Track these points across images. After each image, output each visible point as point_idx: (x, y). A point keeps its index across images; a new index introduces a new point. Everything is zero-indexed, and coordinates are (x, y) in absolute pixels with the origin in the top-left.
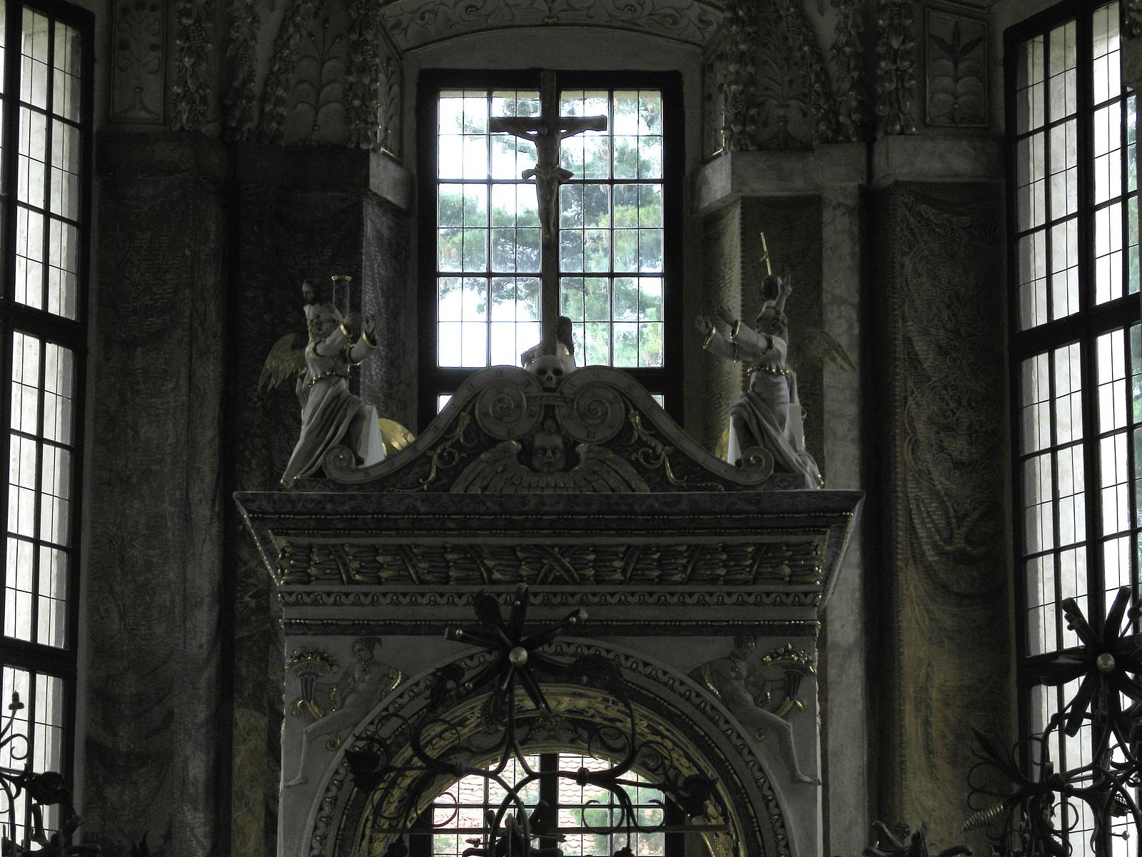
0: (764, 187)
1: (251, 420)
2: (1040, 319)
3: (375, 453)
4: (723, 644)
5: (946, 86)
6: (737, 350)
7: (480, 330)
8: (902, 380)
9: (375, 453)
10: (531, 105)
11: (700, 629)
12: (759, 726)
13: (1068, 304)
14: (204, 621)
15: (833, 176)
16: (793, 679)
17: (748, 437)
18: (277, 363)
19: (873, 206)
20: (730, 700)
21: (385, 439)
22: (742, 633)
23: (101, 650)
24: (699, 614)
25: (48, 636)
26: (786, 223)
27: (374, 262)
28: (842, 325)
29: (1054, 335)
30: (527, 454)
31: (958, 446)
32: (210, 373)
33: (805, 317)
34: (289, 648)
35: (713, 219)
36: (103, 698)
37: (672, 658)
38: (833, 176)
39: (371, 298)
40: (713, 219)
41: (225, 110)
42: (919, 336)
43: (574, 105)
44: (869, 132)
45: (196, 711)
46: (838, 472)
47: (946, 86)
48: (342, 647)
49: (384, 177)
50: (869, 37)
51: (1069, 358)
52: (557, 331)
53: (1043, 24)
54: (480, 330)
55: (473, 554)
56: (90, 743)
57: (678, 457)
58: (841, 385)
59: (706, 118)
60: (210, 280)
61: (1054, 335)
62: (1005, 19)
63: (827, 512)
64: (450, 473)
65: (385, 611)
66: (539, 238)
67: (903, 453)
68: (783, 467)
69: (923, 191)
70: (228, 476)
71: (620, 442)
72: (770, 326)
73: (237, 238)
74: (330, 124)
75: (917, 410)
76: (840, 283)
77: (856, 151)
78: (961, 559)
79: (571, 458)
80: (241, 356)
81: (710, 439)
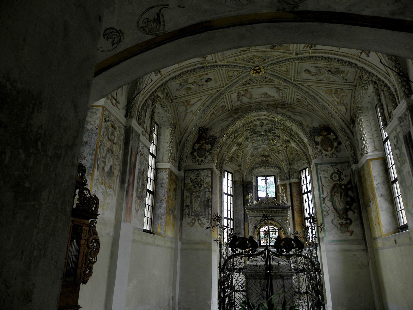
0: (282, 183)
1: (245, 202)
2: (304, 192)
3: (255, 204)
4: (281, 217)
5: (295, 175)
6: (281, 195)
7: (262, 194)
8: (293, 197)
9: (255, 204)
10: (264, 178)
11: (280, 216)
12: (284, 223)
13: (306, 191)
14: (243, 216)
15: (287, 182)
16: (287, 220)
17: (282, 201)
18: (247, 197)
19: (290, 184)
20: (282, 222)
21: (255, 203)
22: (283, 216)
23: (235, 219)
24: (279, 215)
25: (232, 218)
26: (284, 185)
27: (254, 190)
28: (289, 193)
29: (305, 193)
30: (266, 203)
31: (298, 202)
32: (242, 198)
33: (286, 192)
34: (249, 218)
35: (278, 186)
36: (236, 222)
37: (277, 218)
38: (287, 182)
39: (254, 192)
40: (278, 186)
41: (242, 179)
42: (295, 193)
43: (268, 178)
44: (290, 179)
45: (242, 223)
46: (289, 204)
47: (295, 175)
48: (253, 218)
49: (254, 184)
50: (289, 172)
51: (306, 195)
52: (267, 194)
53: (302, 170)
54: (262, 194)
55: (262, 211)
56: (235, 226)
57: (277, 203)
58: (289, 197)
59: (277, 178)
60: (242, 191)
61: (305, 193)
62: (299, 170)
63: (288, 207)
64: (260, 205)
65: (256, 215)
66: (266, 187)
67: (294, 202)
68: (285, 204)
69: (294, 183)
70: (244, 206)
71: (273, 202)
72: (283, 193)
73: (244, 188)
74: (250, 180)
75: (295, 199)
76: (288, 190)
77: (289, 180)
78: (299, 210)
79: (269, 204)
80: (244, 197)
81: (279, 202)
